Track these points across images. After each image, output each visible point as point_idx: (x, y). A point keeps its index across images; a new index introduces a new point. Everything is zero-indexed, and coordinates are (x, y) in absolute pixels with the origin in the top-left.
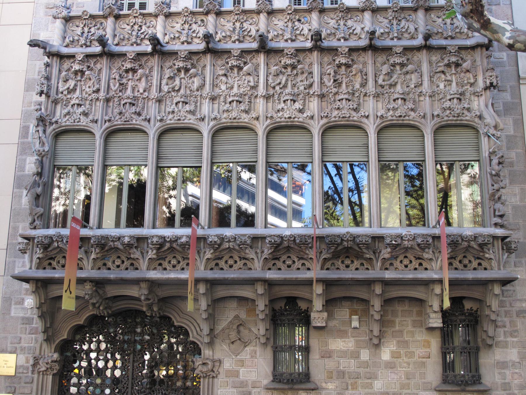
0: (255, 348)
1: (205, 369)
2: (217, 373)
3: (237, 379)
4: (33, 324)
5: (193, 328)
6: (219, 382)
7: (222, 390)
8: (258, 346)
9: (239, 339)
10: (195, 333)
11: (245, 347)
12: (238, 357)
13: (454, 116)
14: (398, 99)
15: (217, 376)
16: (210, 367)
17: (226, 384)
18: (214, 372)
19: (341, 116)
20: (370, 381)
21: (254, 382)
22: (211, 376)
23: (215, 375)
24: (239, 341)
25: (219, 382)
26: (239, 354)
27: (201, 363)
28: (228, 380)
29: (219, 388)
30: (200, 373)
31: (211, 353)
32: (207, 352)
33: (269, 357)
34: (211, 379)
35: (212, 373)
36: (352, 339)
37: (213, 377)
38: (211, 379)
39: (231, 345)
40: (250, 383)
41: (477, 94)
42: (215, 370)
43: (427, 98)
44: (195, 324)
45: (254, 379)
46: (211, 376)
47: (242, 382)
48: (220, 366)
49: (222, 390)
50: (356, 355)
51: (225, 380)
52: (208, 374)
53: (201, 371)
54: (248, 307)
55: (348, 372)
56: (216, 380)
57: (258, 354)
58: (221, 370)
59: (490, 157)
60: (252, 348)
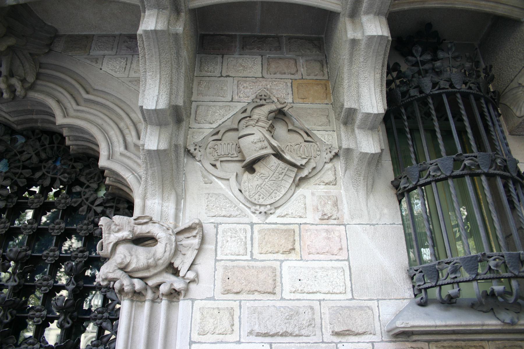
0: (333, 190)
1: (140, 257)
2: (191, 275)
3: (267, 301)
5: (115, 134)
6: (197, 316)
8: (340, 182)
9: (278, 156)
10: (119, 148)
11: (300, 182)
12: (272, 219)
15: (187, 290)
16: (161, 251)
17: (226, 323)
18: (176, 272)
22: (163, 289)
23: (179, 285)
24: (274, 161)
25: (197, 316)
26: (275, 206)
27: (125, 234)
29: (195, 337)
30: (119, 274)
31: (170, 207)
32: (152, 204)
33: (387, 220)
34: (164, 303)
37: (174, 295)
38: (164, 303)
39: (247, 176)
40: (326, 318)
42: (182, 264)
44: (122, 105)
46: (163, 289)
47: (293, 314)
48: (200, 250)
51: (222, 304)
52: (151, 283)
53: (123, 269)
54: (298, 76)
56: (183, 304)
57: (345, 208)
58: (204, 267)
60: (321, 189)
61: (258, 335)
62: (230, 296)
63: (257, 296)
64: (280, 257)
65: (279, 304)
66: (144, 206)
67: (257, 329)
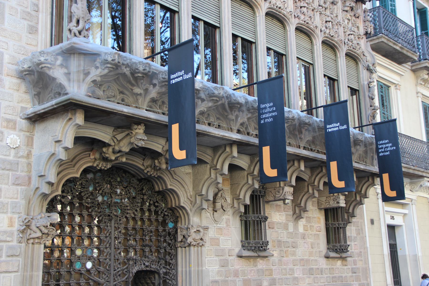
4: (17, 171)
7: (208, 259)
12: (218, 225)
13: (353, 48)
14: (329, 22)
19: (307, 21)
20: (294, 249)
21: (230, 250)
28: (212, 248)
29: (206, 257)
30: (193, 241)
35: (201, 241)
36: (284, 213)
41: (359, 36)
43: (342, 28)
45: (230, 247)
49: (208, 259)
50: (286, 227)
52: (198, 242)
55: (283, 242)
56: (203, 248)
59: (368, 85)
61: (217, 256)
62: (211, 246)
63: (216, 246)
64: (220, 236)
65: (220, 248)
66: (193, 221)
67: (217, 254)
